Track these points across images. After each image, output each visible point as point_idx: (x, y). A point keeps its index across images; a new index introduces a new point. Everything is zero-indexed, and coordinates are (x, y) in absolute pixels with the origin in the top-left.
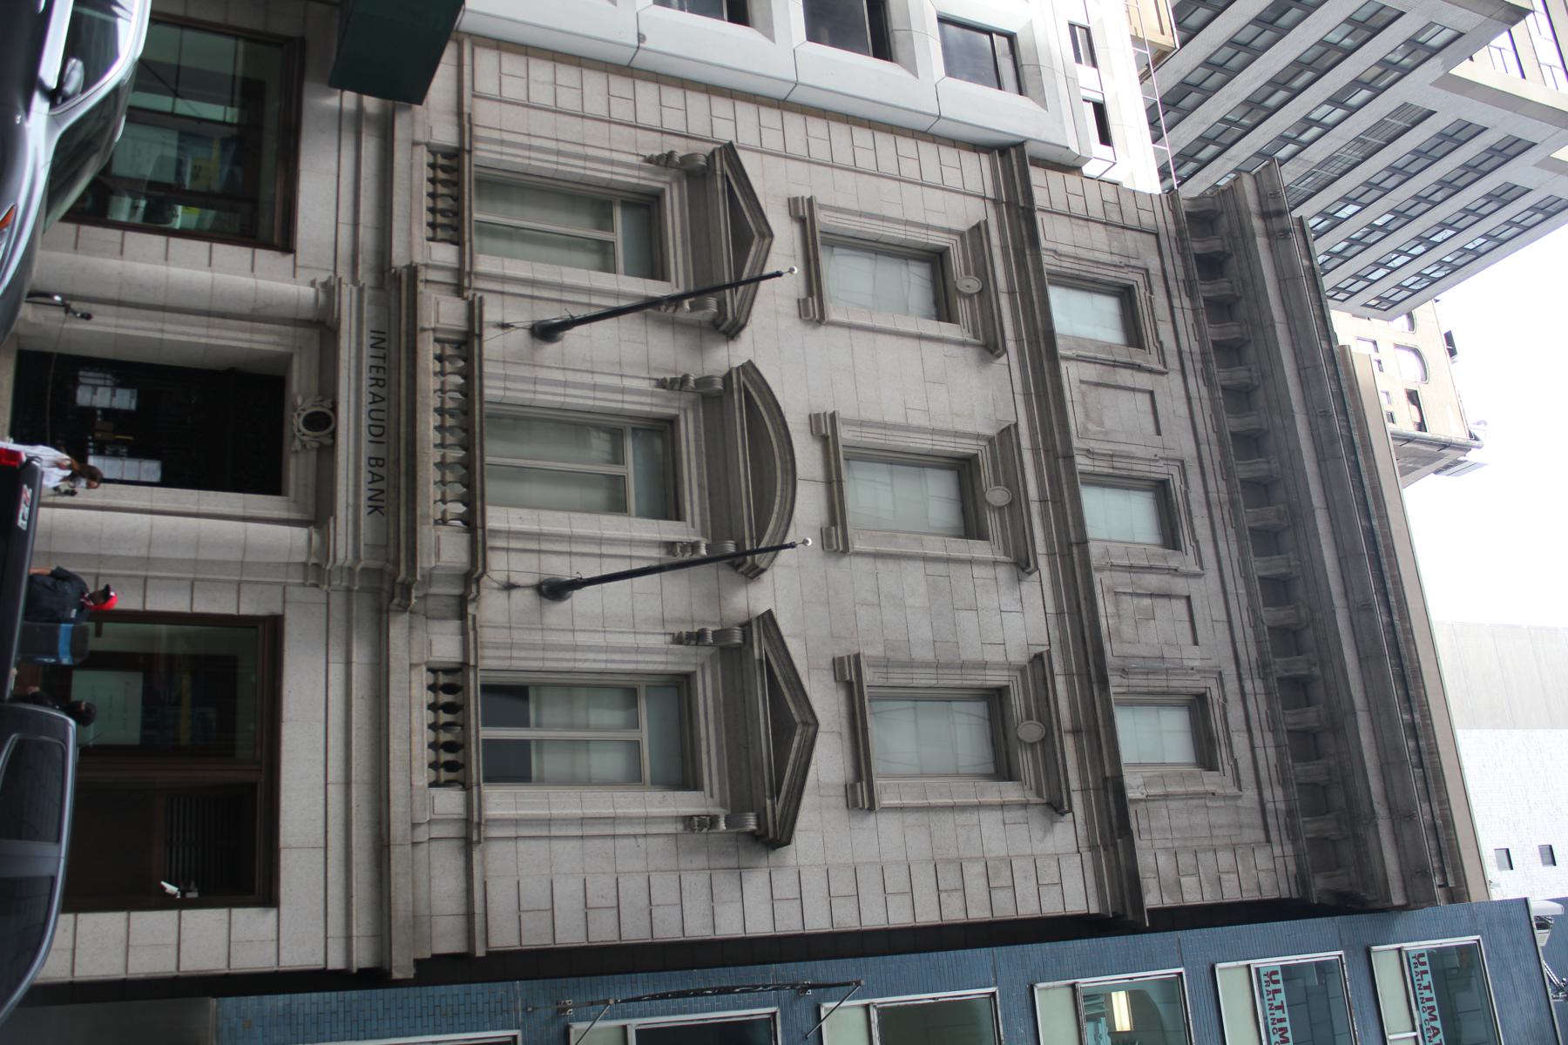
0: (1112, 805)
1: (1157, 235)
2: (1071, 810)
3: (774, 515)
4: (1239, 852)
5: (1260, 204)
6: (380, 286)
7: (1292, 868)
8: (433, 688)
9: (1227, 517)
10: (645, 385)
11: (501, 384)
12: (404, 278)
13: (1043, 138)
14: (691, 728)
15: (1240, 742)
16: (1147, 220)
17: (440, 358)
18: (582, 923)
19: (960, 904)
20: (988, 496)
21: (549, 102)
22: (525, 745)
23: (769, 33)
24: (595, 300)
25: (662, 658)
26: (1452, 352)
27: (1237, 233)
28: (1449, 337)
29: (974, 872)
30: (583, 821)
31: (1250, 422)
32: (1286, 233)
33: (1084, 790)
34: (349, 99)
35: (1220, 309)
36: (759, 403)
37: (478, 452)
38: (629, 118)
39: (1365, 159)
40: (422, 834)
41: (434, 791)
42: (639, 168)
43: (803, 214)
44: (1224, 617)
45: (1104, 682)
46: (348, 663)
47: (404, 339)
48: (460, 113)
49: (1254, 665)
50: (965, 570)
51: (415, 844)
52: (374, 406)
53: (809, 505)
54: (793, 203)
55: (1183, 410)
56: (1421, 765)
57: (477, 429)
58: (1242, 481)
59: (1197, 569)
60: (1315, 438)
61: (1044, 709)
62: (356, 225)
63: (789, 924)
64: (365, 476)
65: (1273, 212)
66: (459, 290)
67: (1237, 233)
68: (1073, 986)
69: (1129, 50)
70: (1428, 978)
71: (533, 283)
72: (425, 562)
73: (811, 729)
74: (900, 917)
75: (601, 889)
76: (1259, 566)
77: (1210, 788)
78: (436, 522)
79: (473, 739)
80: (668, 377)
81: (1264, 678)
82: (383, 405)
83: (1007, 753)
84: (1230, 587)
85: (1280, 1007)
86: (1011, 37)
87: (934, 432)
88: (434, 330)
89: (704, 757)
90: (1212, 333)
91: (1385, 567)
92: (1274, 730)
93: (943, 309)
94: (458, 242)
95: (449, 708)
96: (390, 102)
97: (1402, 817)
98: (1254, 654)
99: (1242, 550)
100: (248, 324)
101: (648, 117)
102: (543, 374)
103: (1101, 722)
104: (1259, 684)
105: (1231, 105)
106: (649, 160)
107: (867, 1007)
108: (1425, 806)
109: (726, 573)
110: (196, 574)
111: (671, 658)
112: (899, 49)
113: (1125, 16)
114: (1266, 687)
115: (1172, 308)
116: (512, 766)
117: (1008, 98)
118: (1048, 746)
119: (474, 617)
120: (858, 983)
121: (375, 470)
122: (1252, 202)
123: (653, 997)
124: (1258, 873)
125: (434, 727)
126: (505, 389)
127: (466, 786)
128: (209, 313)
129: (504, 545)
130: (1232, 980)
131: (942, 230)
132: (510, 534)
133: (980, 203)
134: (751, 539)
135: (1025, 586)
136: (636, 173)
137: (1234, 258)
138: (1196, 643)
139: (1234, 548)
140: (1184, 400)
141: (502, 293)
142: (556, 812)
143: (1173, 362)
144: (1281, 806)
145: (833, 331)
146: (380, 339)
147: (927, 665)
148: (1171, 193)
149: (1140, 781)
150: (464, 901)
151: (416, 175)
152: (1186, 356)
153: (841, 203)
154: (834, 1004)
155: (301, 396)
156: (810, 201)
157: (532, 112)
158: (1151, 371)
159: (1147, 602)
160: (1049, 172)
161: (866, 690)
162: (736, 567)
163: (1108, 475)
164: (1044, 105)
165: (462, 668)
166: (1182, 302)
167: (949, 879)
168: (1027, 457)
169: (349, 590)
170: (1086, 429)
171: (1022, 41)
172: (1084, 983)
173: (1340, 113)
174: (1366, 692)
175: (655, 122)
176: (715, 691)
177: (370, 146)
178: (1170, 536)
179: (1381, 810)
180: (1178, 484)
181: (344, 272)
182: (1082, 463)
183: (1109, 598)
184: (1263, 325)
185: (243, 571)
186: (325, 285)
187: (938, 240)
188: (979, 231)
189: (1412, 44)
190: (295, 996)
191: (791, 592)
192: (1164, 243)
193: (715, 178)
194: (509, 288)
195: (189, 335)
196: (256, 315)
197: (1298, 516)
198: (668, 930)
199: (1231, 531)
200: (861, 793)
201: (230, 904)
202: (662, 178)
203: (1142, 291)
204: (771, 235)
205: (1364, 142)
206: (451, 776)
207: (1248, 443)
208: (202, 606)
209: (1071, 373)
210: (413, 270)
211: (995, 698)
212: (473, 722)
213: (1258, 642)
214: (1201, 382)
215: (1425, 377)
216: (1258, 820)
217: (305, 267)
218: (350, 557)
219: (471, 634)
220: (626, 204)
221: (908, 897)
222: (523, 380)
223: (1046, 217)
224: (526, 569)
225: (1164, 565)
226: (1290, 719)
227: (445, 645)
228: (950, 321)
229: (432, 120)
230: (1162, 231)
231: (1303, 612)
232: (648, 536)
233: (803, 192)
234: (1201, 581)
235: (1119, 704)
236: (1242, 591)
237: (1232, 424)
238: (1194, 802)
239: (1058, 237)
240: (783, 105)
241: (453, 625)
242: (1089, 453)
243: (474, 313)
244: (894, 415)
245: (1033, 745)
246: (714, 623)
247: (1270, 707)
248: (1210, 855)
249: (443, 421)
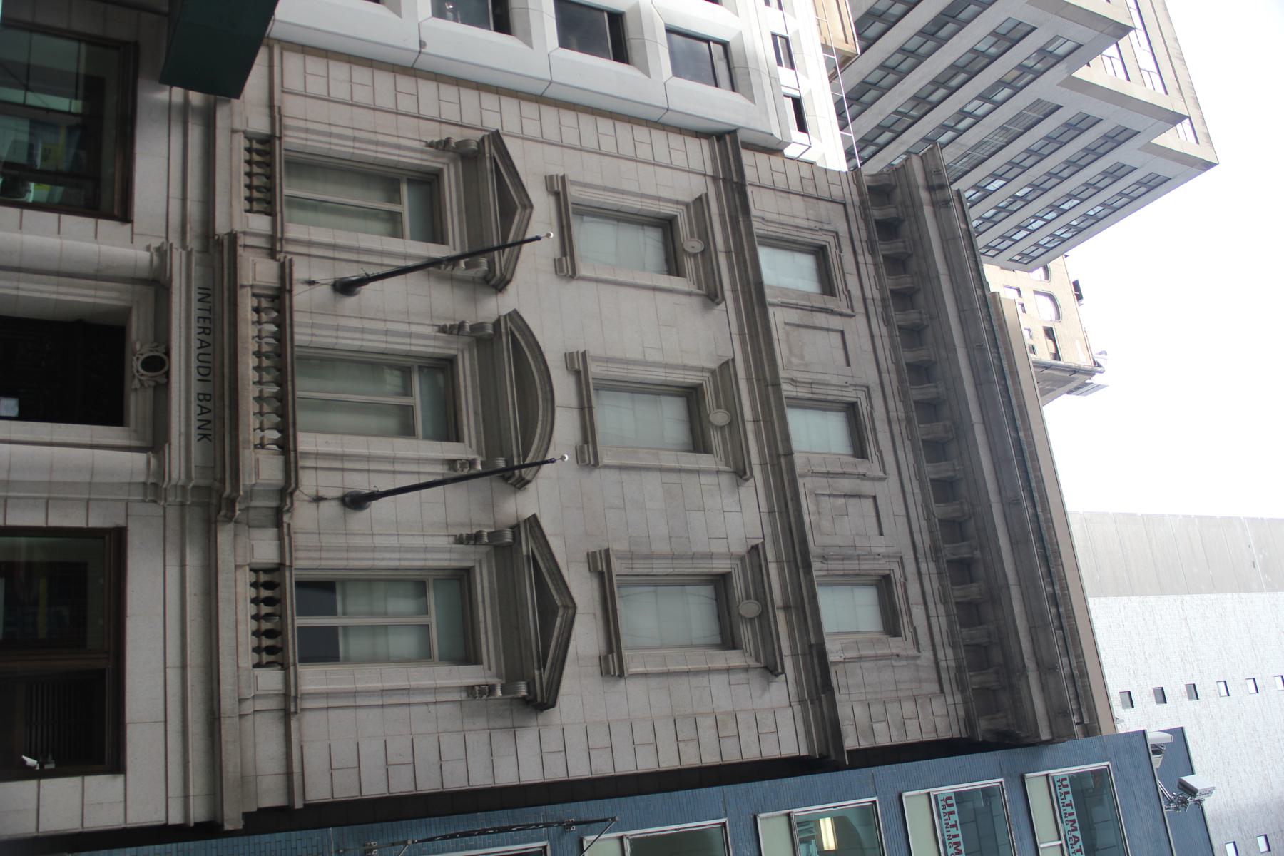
0: (817, 667)
1: (845, 205)
2: (783, 672)
3: (537, 437)
4: (919, 701)
5: (926, 179)
6: (205, 250)
7: (962, 713)
8: (255, 585)
9: (904, 431)
10: (429, 330)
11: (309, 331)
12: (226, 243)
13: (752, 126)
15: (918, 612)
16: (837, 193)
17: (257, 310)
18: (384, 777)
19: (694, 751)
20: (712, 418)
21: (346, 97)
22: (334, 630)
23: (528, 41)
24: (387, 261)
25: (447, 556)
26: (1079, 297)
27: (909, 203)
28: (1076, 285)
29: (706, 725)
30: (383, 692)
31: (921, 355)
32: (947, 202)
34: (177, 94)
35: (896, 264)
37: (290, 388)
38: (413, 110)
39: (1008, 144)
40: (248, 707)
41: (257, 671)
42: (422, 151)
43: (558, 189)
44: (903, 512)
45: (808, 567)
46: (183, 566)
47: (226, 294)
48: (271, 106)
49: (928, 550)
50: (694, 478)
51: (241, 716)
52: (202, 351)
53: (566, 427)
54: (549, 180)
55: (868, 346)
56: (1061, 627)
57: (289, 369)
58: (916, 402)
59: (881, 474)
60: (972, 368)
61: (760, 590)
62: (184, 199)
63: (556, 773)
64: (195, 409)
65: (936, 187)
66: (272, 253)
67: (909, 203)
68: (788, 815)
69: (821, 55)
70: (1070, 797)
71: (334, 247)
72: (247, 480)
73: (570, 612)
74: (647, 764)
75: (399, 749)
76: (930, 471)
77: (895, 651)
78: (255, 447)
79: (290, 627)
80: (448, 323)
81: (936, 561)
82: (209, 350)
83: (731, 627)
85: (954, 826)
86: (725, 45)
87: (666, 366)
88: (252, 286)
89: (483, 636)
90: (889, 283)
91: (1030, 470)
92: (945, 603)
93: (673, 265)
94: (271, 213)
95: (269, 601)
96: (212, 97)
97: (1047, 669)
100: (93, 283)
101: (429, 109)
102: (343, 322)
104: (932, 566)
105: (901, 100)
106: (430, 145)
107: (621, 839)
108: (1065, 660)
109: (498, 484)
110: (50, 494)
111: (454, 556)
112: (634, 53)
113: (816, 28)
114: (938, 568)
115: (857, 263)
116: (323, 648)
117: (722, 95)
119: (289, 525)
120: (613, 819)
122: (920, 179)
123: (445, 837)
124: (936, 718)
125: (256, 617)
126: (313, 335)
127: (284, 666)
128: (58, 274)
129: (314, 465)
130: (916, 805)
131: (670, 201)
132: (317, 455)
133: (702, 178)
135: (743, 490)
136: (419, 156)
137: (906, 223)
138: (881, 534)
140: (868, 338)
141: (309, 255)
142: (360, 686)
143: (859, 306)
144: (952, 663)
145: (583, 284)
146: (206, 295)
147: (664, 557)
148: (855, 171)
149: (839, 647)
150: (284, 762)
152: (869, 302)
153: (588, 180)
154: (594, 837)
155: (139, 342)
156: (563, 178)
157: (332, 105)
158: (841, 314)
159: (841, 501)
160: (758, 154)
161: (615, 578)
162: (506, 479)
163: (809, 399)
164: (752, 100)
165: (279, 568)
166: (866, 259)
167: (686, 731)
168: (743, 385)
169: (182, 505)
170: (790, 362)
171: (734, 48)
172: (797, 812)
173: (987, 106)
175: (434, 114)
176: (490, 582)
177: (195, 134)
178: (859, 450)
179: (1030, 665)
180: (864, 405)
181: (175, 239)
182: (787, 390)
183: (811, 499)
184: (929, 277)
185: (91, 492)
186: (158, 249)
187: (667, 209)
188: (701, 202)
189: (1043, 52)
190: (140, 848)
191: (553, 498)
192: (850, 210)
193: (485, 160)
195: (41, 292)
196: (99, 275)
197: (960, 430)
198: (455, 781)
199: (907, 443)
200: (612, 662)
201: (83, 773)
203: (833, 249)
204: (532, 206)
205: (1008, 130)
206: (272, 658)
207: (920, 372)
208: (56, 521)
209: (777, 317)
210: (233, 237)
211: (720, 582)
212: (289, 612)
213: (931, 532)
214: (881, 323)
215: (1058, 317)
216: (934, 676)
218: (183, 476)
219: (287, 539)
220: (411, 182)
221: (653, 747)
222: (327, 327)
223: (755, 190)
224: (332, 484)
225: (855, 471)
226: (957, 593)
227: (265, 549)
228: (678, 275)
229: (247, 112)
230: (849, 201)
231: (966, 508)
234: (885, 484)
235: (821, 584)
236: (917, 491)
237: (907, 356)
238: (882, 662)
239: (764, 207)
240: (540, 99)
241: (272, 532)
242: (793, 381)
243: (285, 272)
244: (634, 353)
245: (751, 620)
246: (489, 526)
247: (941, 584)
248: (896, 704)
249: (260, 362)
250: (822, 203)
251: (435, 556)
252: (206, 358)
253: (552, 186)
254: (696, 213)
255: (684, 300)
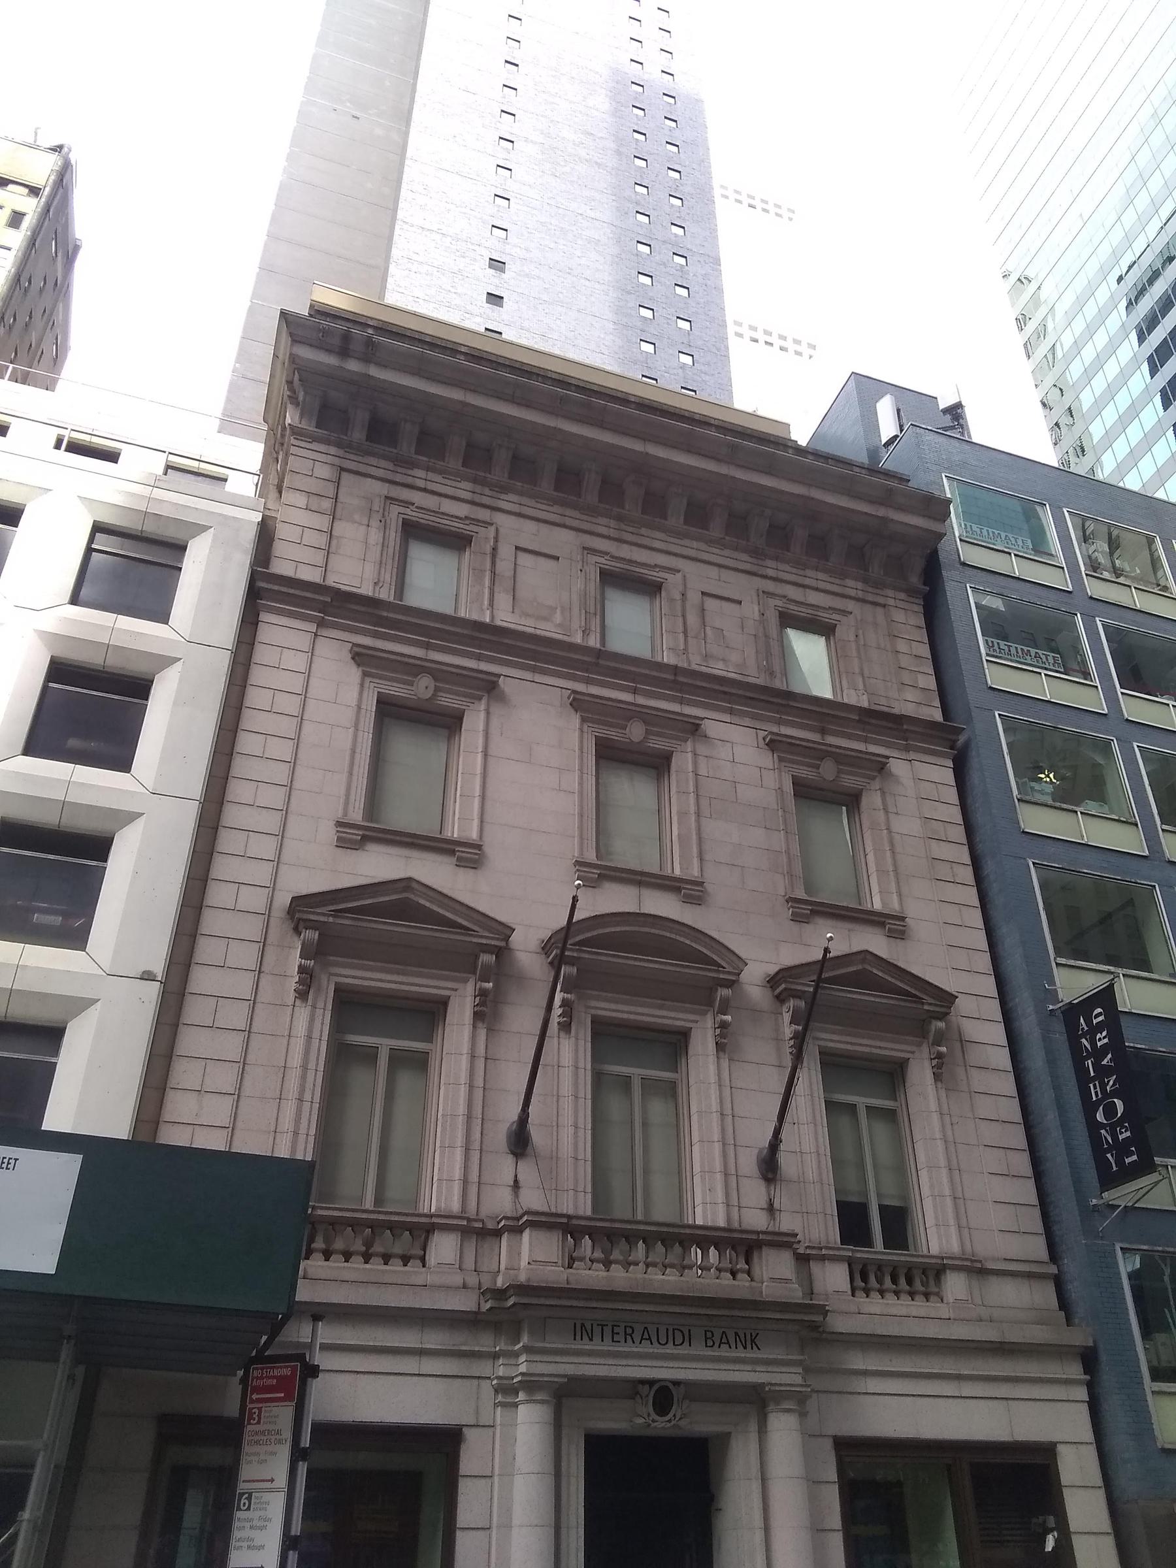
0: (879, 722)
1: (342, 469)
2: (888, 757)
3: (694, 945)
5: (329, 351)
7: (902, 596)
9: (631, 529)
14: (841, 1056)
15: (814, 598)
16: (324, 471)
20: (636, 740)
22: (883, 1209)
25: (813, 1073)
32: (369, 342)
33: (866, 740)
36: (589, 935)
42: (314, 1007)
43: (357, 835)
44: (716, 569)
46: (865, 1373)
52: (654, 1340)
54: (343, 843)
55: (530, 526)
57: (665, 1229)
59: (679, 575)
64: (724, 1352)
73: (869, 957)
77: (852, 638)
79: (884, 1257)
82: (652, 1330)
83: (834, 792)
84: (692, 553)
86: (98, 528)
90: (454, 463)
92: (805, 567)
94: (423, 1230)
98: (745, 557)
99: (659, 529)
103: (818, 709)
104: (769, 563)
112: (136, 667)
116: (898, 1222)
118: (844, 759)
119: (807, 1247)
121: (717, 1344)
133: (320, 640)
134: (718, 971)
135: (710, 733)
136: (319, 1012)
139: (658, 535)
140: (522, 520)
143: (483, 514)
144: (860, 585)
145: (485, 839)
146: (582, 1330)
149: (853, 692)
151: (347, 1275)
152: (477, 498)
156: (339, 824)
157: (239, 1124)
158: (496, 540)
159: (709, 630)
165: (851, 1263)
167: (944, 871)
168: (595, 690)
170: (560, 625)
174: (794, 481)
179: (881, 512)
187: (370, 704)
193: (327, 925)
194: (474, 1176)
197: (642, 467)
199: (643, 531)
202: (324, 982)
203: (408, 511)
204: (410, 879)
209: (505, 617)
213: (736, 549)
214: (503, 496)
216: (868, 607)
217: (477, 1412)
224: (755, 1192)
225: (679, 602)
227: (834, 1278)
228: (461, 719)
232: (712, 1068)
233: (328, 833)
236: (695, 544)
237: (546, 485)
245: (839, 771)
249: (617, 1262)
250: (341, 498)
251: (815, 1088)
252: (662, 1333)
253: (351, 841)
254: (377, 668)
255: (495, 722)
